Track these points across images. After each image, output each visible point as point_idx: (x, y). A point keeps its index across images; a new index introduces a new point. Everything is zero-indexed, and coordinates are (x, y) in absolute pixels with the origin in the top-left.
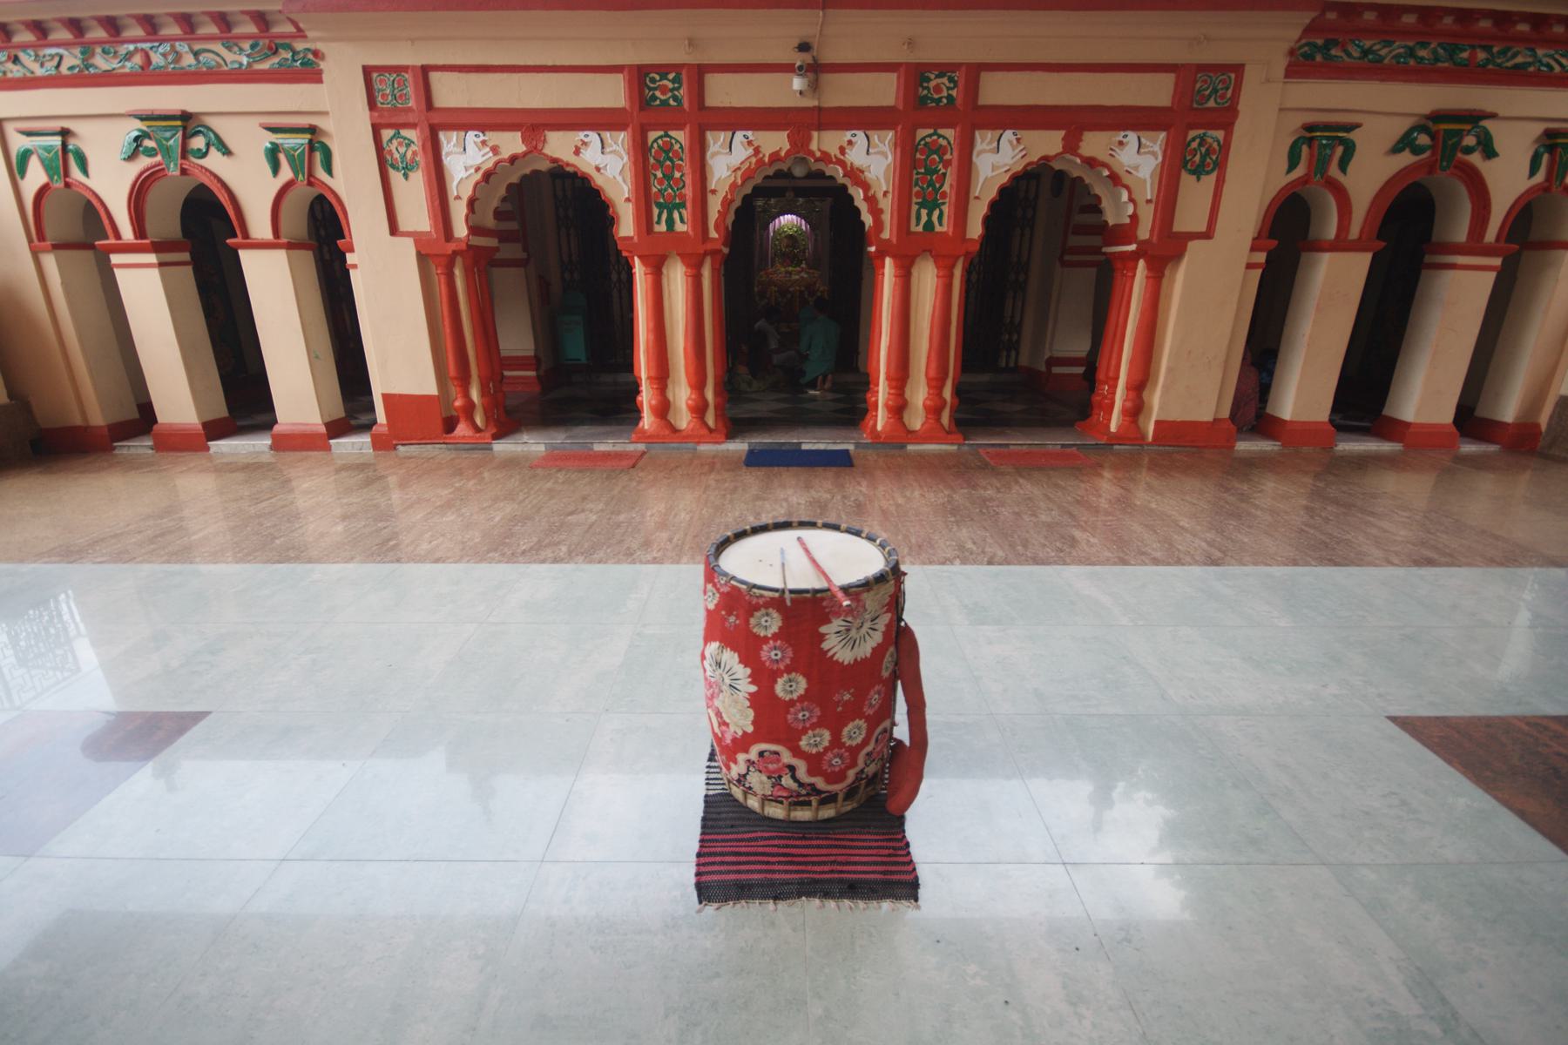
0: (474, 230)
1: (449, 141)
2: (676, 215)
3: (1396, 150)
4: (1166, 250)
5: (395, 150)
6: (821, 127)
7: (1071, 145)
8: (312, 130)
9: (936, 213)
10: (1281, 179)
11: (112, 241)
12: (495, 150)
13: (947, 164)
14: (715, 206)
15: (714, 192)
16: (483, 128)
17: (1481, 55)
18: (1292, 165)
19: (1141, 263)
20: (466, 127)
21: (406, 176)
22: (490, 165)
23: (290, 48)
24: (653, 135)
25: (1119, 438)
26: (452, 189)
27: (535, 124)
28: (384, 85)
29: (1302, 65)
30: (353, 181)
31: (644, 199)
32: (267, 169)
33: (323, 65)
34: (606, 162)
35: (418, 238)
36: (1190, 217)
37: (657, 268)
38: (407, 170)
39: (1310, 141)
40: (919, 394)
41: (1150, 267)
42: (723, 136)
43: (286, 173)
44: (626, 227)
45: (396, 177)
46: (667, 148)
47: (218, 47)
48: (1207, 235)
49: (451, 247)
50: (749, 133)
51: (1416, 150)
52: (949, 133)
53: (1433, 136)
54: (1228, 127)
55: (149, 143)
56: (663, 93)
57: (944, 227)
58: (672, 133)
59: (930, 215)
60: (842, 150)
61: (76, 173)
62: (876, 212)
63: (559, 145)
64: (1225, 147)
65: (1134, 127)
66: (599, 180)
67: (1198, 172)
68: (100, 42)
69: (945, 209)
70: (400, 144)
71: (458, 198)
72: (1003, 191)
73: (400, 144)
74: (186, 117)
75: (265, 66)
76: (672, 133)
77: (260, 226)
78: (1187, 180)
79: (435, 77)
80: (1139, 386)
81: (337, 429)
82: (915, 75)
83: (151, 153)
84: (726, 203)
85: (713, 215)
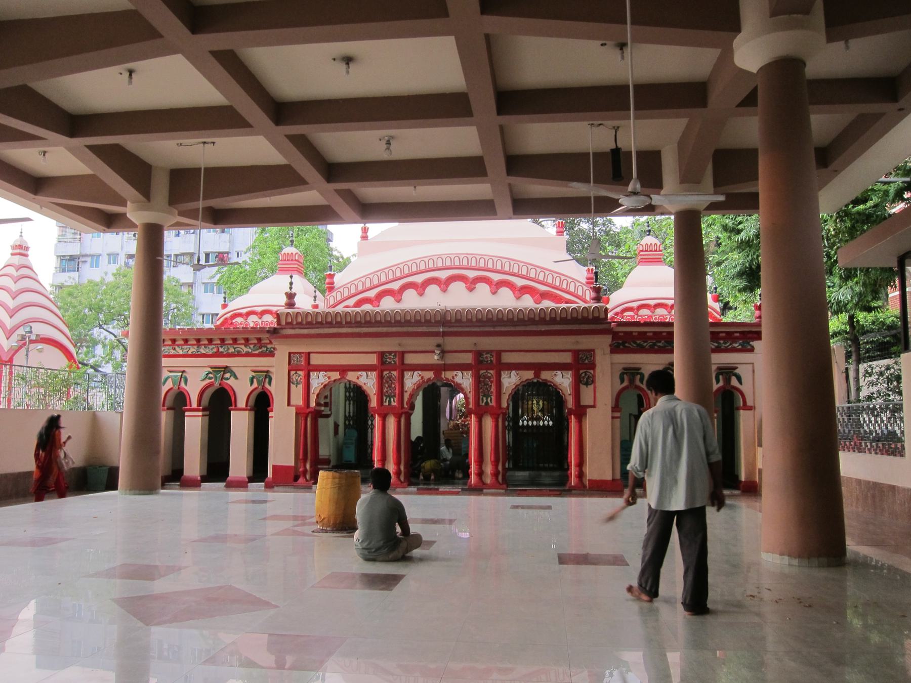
0: (318, 404)
4: (580, 412)
5: (294, 378)
8: (268, 372)
11: (188, 407)
12: (329, 378)
13: (492, 382)
16: (326, 371)
18: (622, 381)
20: (320, 371)
24: (385, 373)
25: (574, 488)
26: (312, 391)
28: (295, 359)
29: (616, 349)
30: (277, 390)
31: (381, 394)
34: (368, 382)
36: (586, 399)
37: (384, 418)
38: (298, 383)
40: (488, 469)
41: (576, 418)
42: (410, 373)
43: (255, 385)
44: (374, 403)
45: (293, 386)
46: (390, 377)
47: (243, 347)
48: (594, 406)
49: (309, 410)
52: (492, 372)
55: (211, 375)
57: (493, 404)
61: (183, 384)
64: (594, 376)
66: (365, 388)
67: (587, 384)
68: (204, 345)
74: (227, 367)
75: (257, 352)
77: (241, 403)
78: (583, 387)
79: (312, 355)
80: (581, 464)
81: (252, 479)
82: (478, 354)
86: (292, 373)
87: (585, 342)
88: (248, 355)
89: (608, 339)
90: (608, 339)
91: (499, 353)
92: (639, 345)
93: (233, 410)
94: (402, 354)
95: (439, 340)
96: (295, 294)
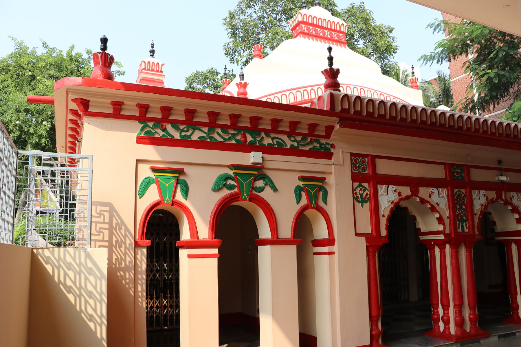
12: (400, 194)
19: (448, 246)
22: (397, 200)
23: (318, 142)
26: (382, 212)
47: (285, 138)
50: (484, 191)
55: (230, 182)
56: (457, 174)
58: (461, 190)
70: (361, 190)
73: (361, 190)
75: (307, 148)
76: (362, 184)
79: (378, 161)
83: (231, 187)
84: (479, 219)
88: (294, 152)
96: (338, 71)
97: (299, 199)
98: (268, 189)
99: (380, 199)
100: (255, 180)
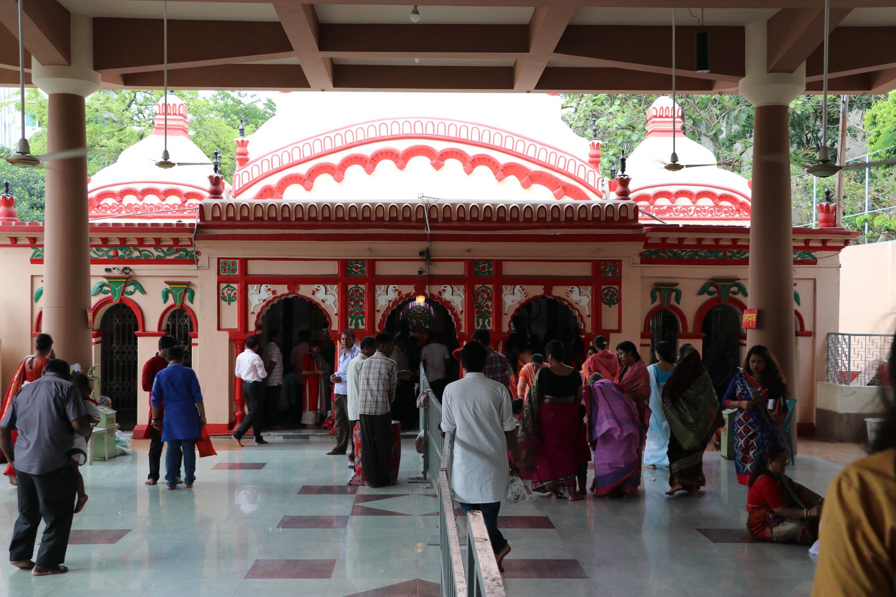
0: (258, 327)
1: (252, 289)
2: (360, 321)
3: (701, 292)
6: (430, 284)
7: (548, 290)
8: (188, 283)
9: (487, 321)
10: (650, 306)
12: (274, 292)
14: (379, 317)
15: (378, 311)
17: (729, 254)
18: (653, 301)
21: (229, 304)
24: (350, 287)
26: (251, 309)
27: (294, 281)
29: (646, 260)
30: (203, 306)
31: (344, 314)
32: (161, 300)
33: (199, 257)
34: (328, 298)
35: (232, 332)
38: (230, 301)
39: (660, 291)
42: (383, 287)
44: (335, 326)
45: (224, 304)
47: (152, 250)
48: (619, 331)
51: (710, 293)
52: (490, 286)
53: (717, 287)
54: (620, 284)
55: (106, 288)
59: (483, 322)
60: (440, 293)
62: (458, 320)
63: (305, 290)
65: (578, 285)
66: (323, 305)
67: (610, 303)
69: (491, 319)
71: (253, 313)
72: (518, 310)
75: (172, 257)
77: (152, 324)
78: (605, 307)
79: (249, 262)
82: (471, 264)
83: (106, 292)
85: (377, 322)
86: (223, 285)
87: (609, 251)
88: (159, 261)
89: (639, 247)
90: (639, 247)
91: (498, 264)
92: (675, 254)
93: (141, 335)
94: (372, 264)
95: (423, 245)
97: (166, 299)
98: (138, 292)
99: (250, 297)
100: (125, 286)
